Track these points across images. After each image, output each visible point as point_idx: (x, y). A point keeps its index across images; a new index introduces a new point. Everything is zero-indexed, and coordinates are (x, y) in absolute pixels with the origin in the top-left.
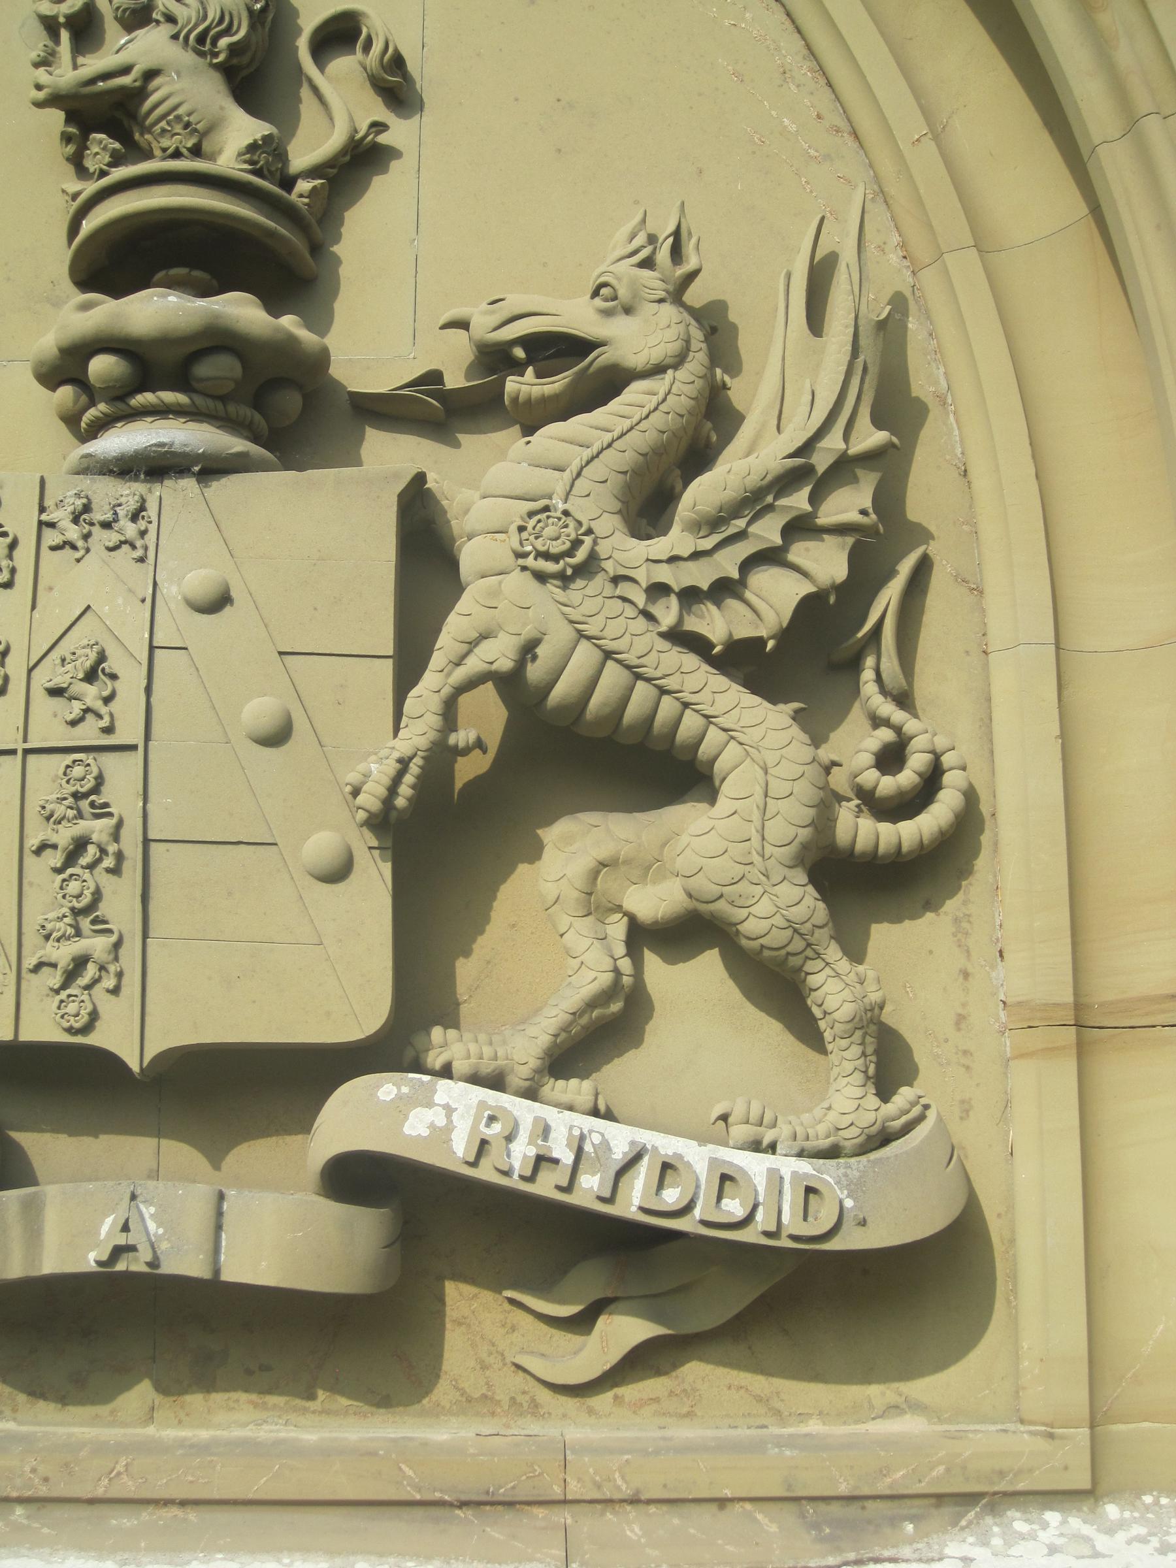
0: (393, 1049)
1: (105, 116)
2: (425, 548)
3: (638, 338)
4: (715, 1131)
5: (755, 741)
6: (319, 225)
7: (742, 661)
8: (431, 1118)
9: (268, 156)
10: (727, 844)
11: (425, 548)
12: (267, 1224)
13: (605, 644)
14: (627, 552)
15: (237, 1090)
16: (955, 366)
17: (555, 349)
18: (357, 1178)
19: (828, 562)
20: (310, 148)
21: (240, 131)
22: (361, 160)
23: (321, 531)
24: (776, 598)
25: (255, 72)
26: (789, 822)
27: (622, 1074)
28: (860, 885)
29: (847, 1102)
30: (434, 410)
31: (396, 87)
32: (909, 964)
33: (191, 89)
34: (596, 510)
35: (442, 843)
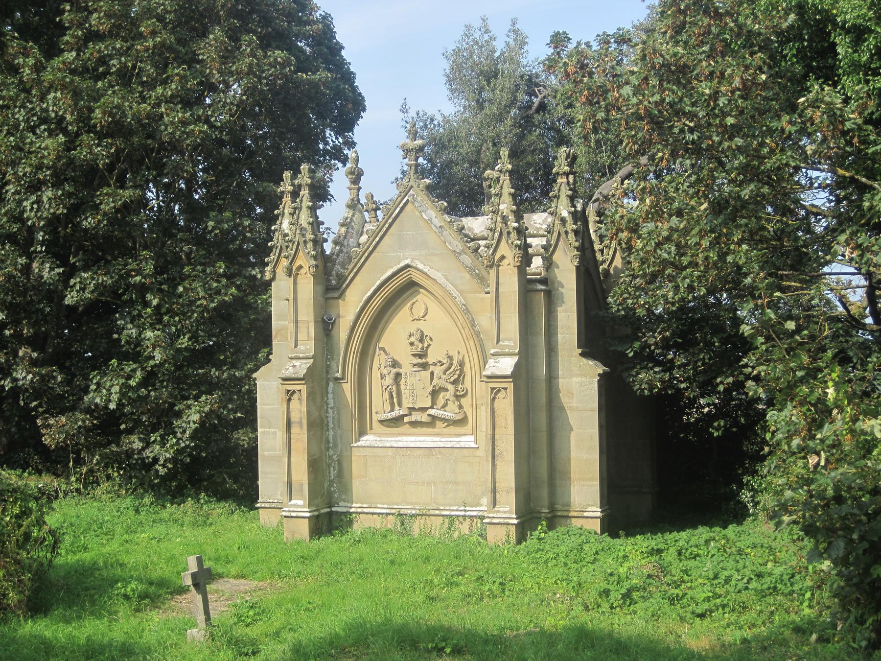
0: (432, 407)
1: (412, 344)
2: (432, 373)
3: (444, 361)
4: (451, 413)
5: (451, 388)
6: (426, 351)
7: (453, 383)
8: (432, 412)
9: (422, 348)
10: (449, 394)
11: (432, 373)
12: (424, 418)
13: (441, 383)
14: (444, 377)
15: (423, 409)
16: (467, 360)
17: (440, 362)
18: (429, 415)
19: (456, 376)
20: (426, 345)
21: (420, 346)
22: (429, 345)
23: (427, 374)
24: (452, 379)
25: (421, 340)
26: (452, 393)
27: (446, 408)
28: (458, 397)
29: (457, 410)
30: (435, 364)
31: (431, 339)
32: (463, 401)
33: (416, 343)
34: (441, 374)
35: (434, 394)
